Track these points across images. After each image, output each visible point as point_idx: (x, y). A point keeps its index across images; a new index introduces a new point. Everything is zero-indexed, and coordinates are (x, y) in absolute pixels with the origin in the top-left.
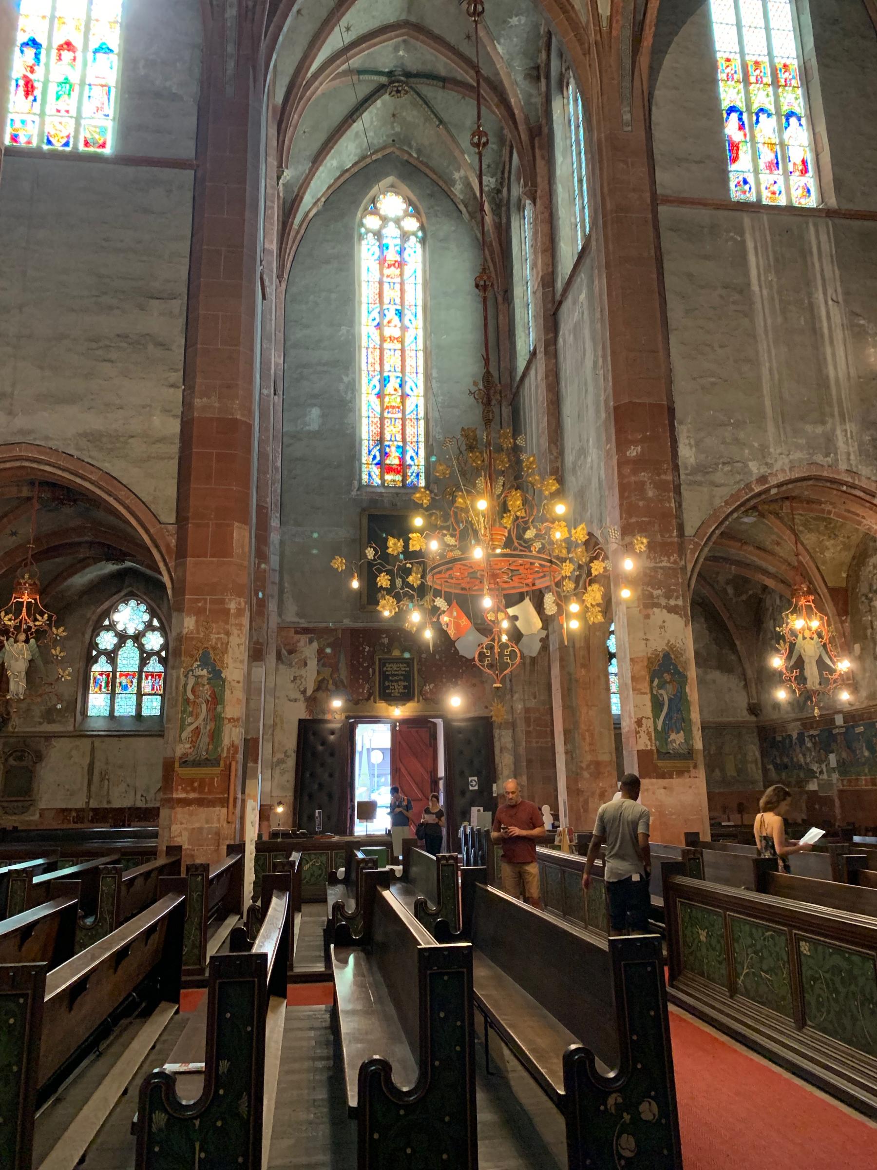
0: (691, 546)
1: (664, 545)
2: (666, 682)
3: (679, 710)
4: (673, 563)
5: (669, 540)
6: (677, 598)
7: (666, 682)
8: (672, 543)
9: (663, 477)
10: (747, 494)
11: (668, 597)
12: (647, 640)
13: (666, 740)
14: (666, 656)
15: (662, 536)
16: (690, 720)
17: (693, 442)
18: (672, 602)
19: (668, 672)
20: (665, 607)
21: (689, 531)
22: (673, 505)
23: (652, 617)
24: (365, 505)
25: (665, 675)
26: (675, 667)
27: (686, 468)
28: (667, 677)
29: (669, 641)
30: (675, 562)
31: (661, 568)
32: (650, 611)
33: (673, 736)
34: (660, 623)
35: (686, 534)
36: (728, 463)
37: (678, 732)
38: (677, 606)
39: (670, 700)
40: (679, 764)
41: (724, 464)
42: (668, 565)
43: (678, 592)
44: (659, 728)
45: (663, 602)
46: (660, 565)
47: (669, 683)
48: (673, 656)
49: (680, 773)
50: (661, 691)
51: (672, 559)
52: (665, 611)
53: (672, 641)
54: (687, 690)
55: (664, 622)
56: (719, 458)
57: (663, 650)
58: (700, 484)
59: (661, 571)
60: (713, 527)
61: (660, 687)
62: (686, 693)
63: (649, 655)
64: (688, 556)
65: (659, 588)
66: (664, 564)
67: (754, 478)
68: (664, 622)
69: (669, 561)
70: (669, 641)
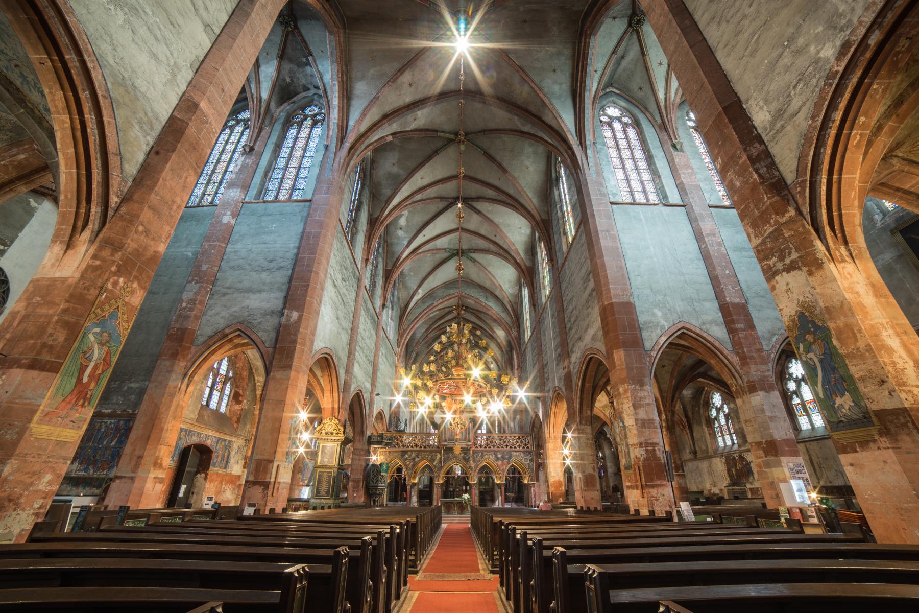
0: (799, 189)
1: (762, 214)
2: (811, 344)
3: (834, 369)
4: (774, 225)
5: (764, 208)
6: (790, 253)
7: (811, 344)
8: (767, 209)
9: (741, 161)
10: (831, 85)
11: (782, 258)
12: (781, 310)
13: (833, 406)
14: (801, 315)
15: (758, 210)
16: (851, 377)
17: (761, 103)
18: (788, 261)
19: (809, 332)
20: (784, 270)
21: (790, 177)
22: (755, 176)
23: (777, 286)
24: (893, 226)
25: (807, 336)
26: (813, 323)
27: (765, 129)
28: (809, 338)
29: (798, 300)
30: (776, 222)
31: (767, 237)
32: (774, 282)
33: (839, 401)
34: (785, 287)
35: (789, 182)
36: (800, 80)
37: (842, 395)
38: (792, 262)
39: (821, 361)
40: (859, 433)
41: (795, 87)
42: (772, 229)
43: (788, 247)
44: (821, 396)
45: (780, 266)
46: (766, 234)
47: (813, 343)
48: (807, 314)
49: (865, 444)
50: (809, 356)
51: (772, 221)
52: (785, 274)
53: (801, 299)
54: (835, 342)
55: (788, 284)
56: (789, 88)
57: (797, 312)
58: (783, 127)
59: (769, 240)
60: (812, 153)
61: (807, 352)
62: (835, 347)
63: (787, 324)
64: (800, 201)
65: (773, 256)
66: (768, 232)
67: (833, 60)
68: (788, 284)
69: (771, 226)
70: (798, 300)
